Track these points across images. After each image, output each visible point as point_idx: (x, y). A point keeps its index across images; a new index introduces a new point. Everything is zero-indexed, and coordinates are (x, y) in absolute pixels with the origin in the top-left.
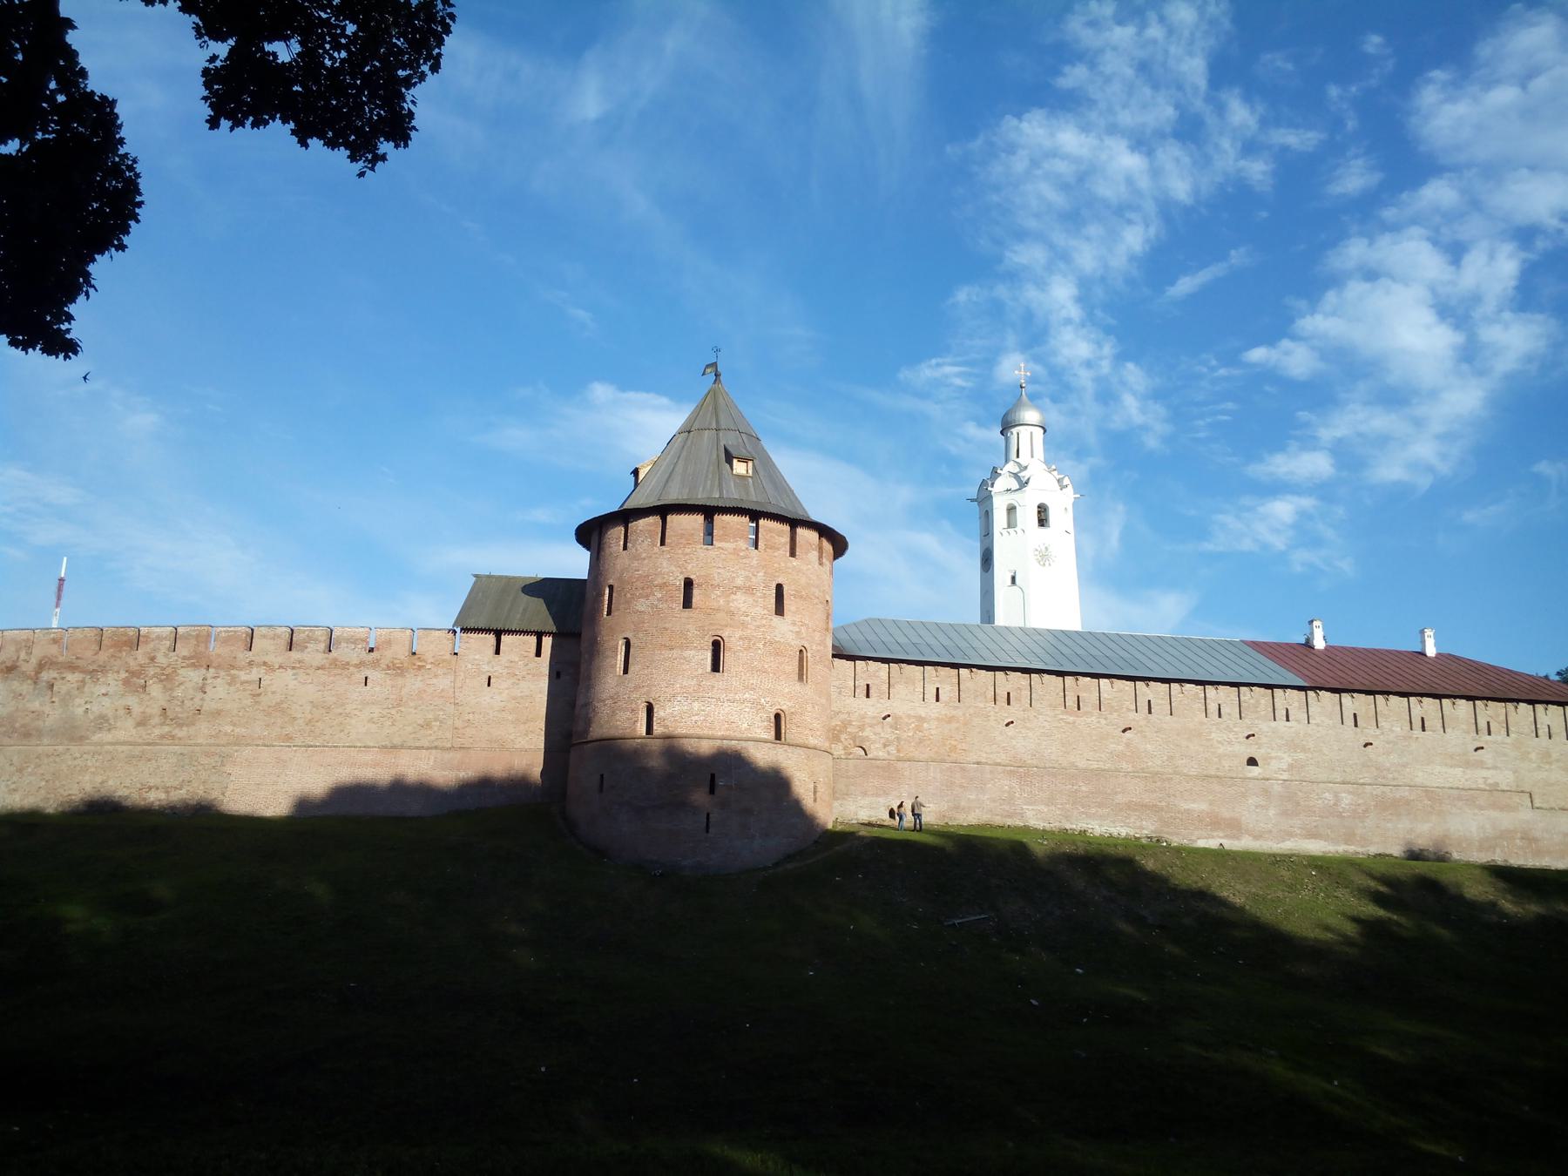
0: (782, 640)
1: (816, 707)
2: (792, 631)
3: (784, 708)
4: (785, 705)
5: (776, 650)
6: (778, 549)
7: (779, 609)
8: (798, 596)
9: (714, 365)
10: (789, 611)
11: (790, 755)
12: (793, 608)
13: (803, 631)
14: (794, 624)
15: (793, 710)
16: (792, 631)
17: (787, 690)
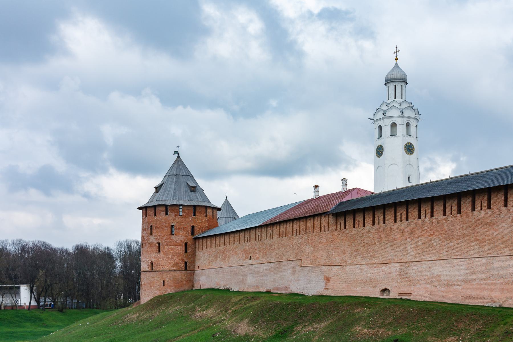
0: (152, 242)
1: (164, 259)
2: (154, 239)
3: (153, 261)
4: (153, 260)
5: (151, 245)
6: (151, 215)
7: (151, 234)
8: (157, 227)
9: (177, 152)
10: (154, 233)
11: (154, 274)
12: (155, 232)
13: (158, 238)
14: (155, 236)
15: (155, 261)
16: (154, 239)
17: (153, 256)
